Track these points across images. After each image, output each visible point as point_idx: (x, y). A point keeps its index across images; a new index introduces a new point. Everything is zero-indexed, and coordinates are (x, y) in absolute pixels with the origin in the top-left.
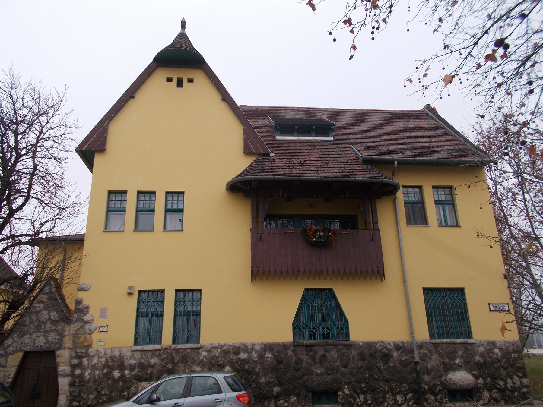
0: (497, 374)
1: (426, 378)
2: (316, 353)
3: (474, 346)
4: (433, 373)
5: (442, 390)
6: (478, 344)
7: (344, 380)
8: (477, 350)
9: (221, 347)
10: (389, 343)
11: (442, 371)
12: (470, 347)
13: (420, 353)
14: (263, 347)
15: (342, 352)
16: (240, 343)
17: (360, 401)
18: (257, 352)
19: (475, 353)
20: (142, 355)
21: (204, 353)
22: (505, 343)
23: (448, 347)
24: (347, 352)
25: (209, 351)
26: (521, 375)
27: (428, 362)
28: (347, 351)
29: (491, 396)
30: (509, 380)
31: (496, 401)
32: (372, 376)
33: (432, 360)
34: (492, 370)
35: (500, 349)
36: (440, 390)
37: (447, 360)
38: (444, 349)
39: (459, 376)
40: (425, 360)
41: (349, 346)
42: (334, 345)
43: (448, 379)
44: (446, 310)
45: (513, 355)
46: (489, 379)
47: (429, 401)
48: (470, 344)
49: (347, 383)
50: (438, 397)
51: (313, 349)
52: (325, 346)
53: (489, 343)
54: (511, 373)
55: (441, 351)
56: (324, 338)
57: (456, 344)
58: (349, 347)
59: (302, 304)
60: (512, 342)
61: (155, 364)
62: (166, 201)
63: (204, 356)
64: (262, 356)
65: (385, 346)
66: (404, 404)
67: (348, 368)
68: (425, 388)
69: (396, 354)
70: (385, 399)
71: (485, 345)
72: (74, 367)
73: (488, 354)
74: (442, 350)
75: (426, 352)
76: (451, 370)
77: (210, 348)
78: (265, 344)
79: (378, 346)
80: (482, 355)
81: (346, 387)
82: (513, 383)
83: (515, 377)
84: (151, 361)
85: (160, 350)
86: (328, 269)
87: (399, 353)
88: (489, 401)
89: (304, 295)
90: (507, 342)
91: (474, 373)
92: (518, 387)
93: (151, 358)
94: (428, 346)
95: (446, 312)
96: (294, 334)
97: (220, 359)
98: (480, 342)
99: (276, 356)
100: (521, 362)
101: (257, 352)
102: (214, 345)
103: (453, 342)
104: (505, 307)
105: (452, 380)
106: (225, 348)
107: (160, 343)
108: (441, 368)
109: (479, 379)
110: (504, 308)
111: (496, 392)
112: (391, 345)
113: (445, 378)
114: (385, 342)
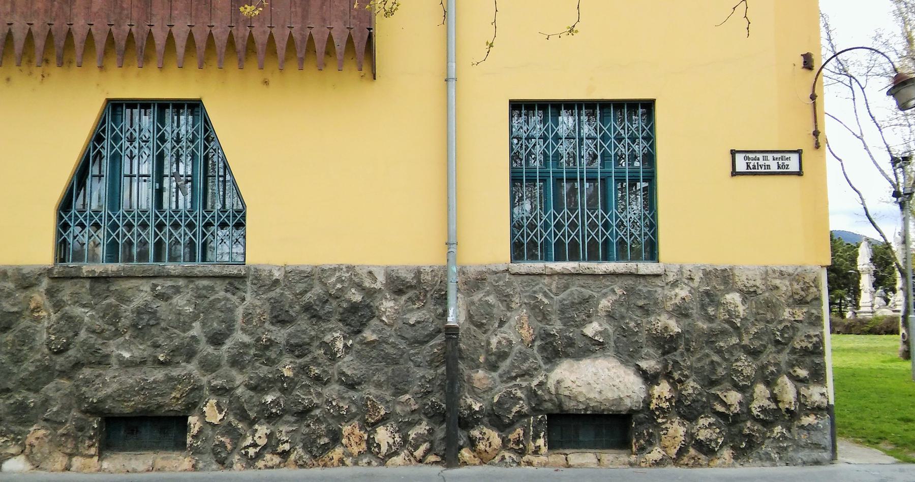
0: (721, 371)
1: (480, 376)
2: (123, 299)
3: (658, 282)
4: (505, 365)
5: (526, 416)
6: (671, 278)
7: (209, 382)
8: (666, 296)
10: (370, 273)
11: (536, 359)
12: (642, 287)
13: (473, 303)
15: (212, 298)
17: (255, 445)
19: (656, 304)
22: (767, 272)
23: (566, 287)
24: (228, 300)
26: (803, 373)
27: (495, 331)
28: (229, 295)
29: (690, 435)
30: (761, 390)
31: (707, 449)
32: (303, 369)
33: (506, 325)
34: (707, 355)
35: (748, 294)
36: (520, 415)
37: (556, 326)
38: (554, 290)
39: (589, 375)
40: (482, 324)
42: (186, 277)
43: (551, 384)
44: (582, 172)
45: (786, 314)
46: (692, 384)
47: (481, 446)
48: (644, 276)
49: (219, 391)
50: (512, 436)
51: (113, 288)
52: (155, 281)
53: (707, 274)
54: (773, 368)
55: (540, 296)
57: (594, 275)
58: (236, 284)
59: (95, 148)
60: (791, 271)
65: (357, 280)
66: (396, 453)
67: (225, 347)
68: (470, 407)
69: (391, 304)
70: (336, 438)
71: (697, 279)
73: (703, 307)
74: (546, 295)
75: (491, 299)
76: (567, 356)
79: (333, 279)
80: (681, 312)
81: (213, 401)
82: (774, 398)
83: (784, 380)
86: (253, 33)
87: (402, 302)
88: (682, 452)
89: (104, 122)
90: (774, 271)
91: (644, 365)
92: (788, 410)
94: (501, 283)
95: (582, 179)
98: (681, 271)
100: (812, 333)
103: (587, 271)
104: (786, 162)
105: (563, 385)
108: (535, 348)
109: (658, 384)
110: (784, 166)
111: (710, 424)
112: (375, 280)
113: (541, 378)
114: (357, 269)
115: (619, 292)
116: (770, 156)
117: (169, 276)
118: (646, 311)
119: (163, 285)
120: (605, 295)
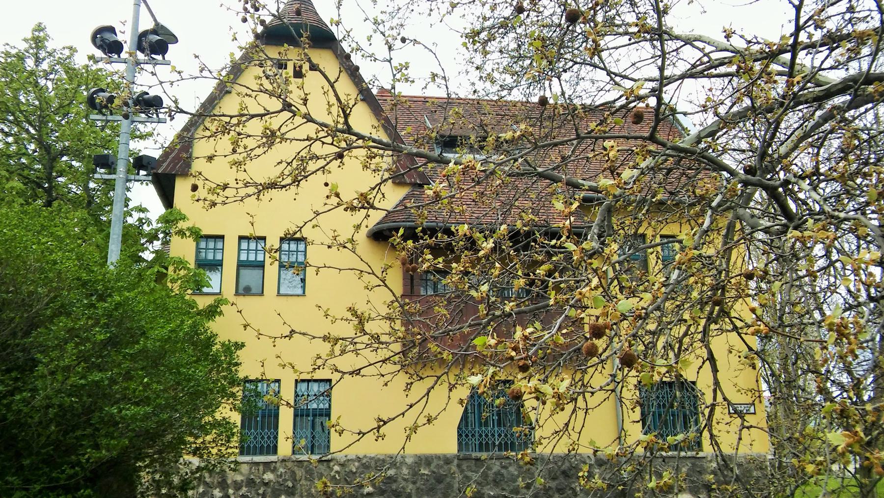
2: (489, 468)
3: (704, 460)
6: (709, 459)
9: (359, 459)
14: (417, 460)
18: (410, 467)
20: (251, 469)
21: (337, 468)
25: (342, 465)
35: (740, 465)
45: (755, 474)
55: (658, 467)
56: (500, 450)
61: (270, 481)
62: (240, 250)
63: (337, 472)
64: (415, 474)
77: (345, 461)
78: (419, 457)
84: (264, 477)
85: (276, 462)
93: (264, 473)
96: (460, 444)
97: (357, 475)
99: (434, 472)
101: (410, 467)
102: (349, 457)
106: (364, 461)
107: (275, 451)
115: (690, 465)
116: (743, 406)
118: (700, 473)
119: (505, 462)
120: (684, 466)
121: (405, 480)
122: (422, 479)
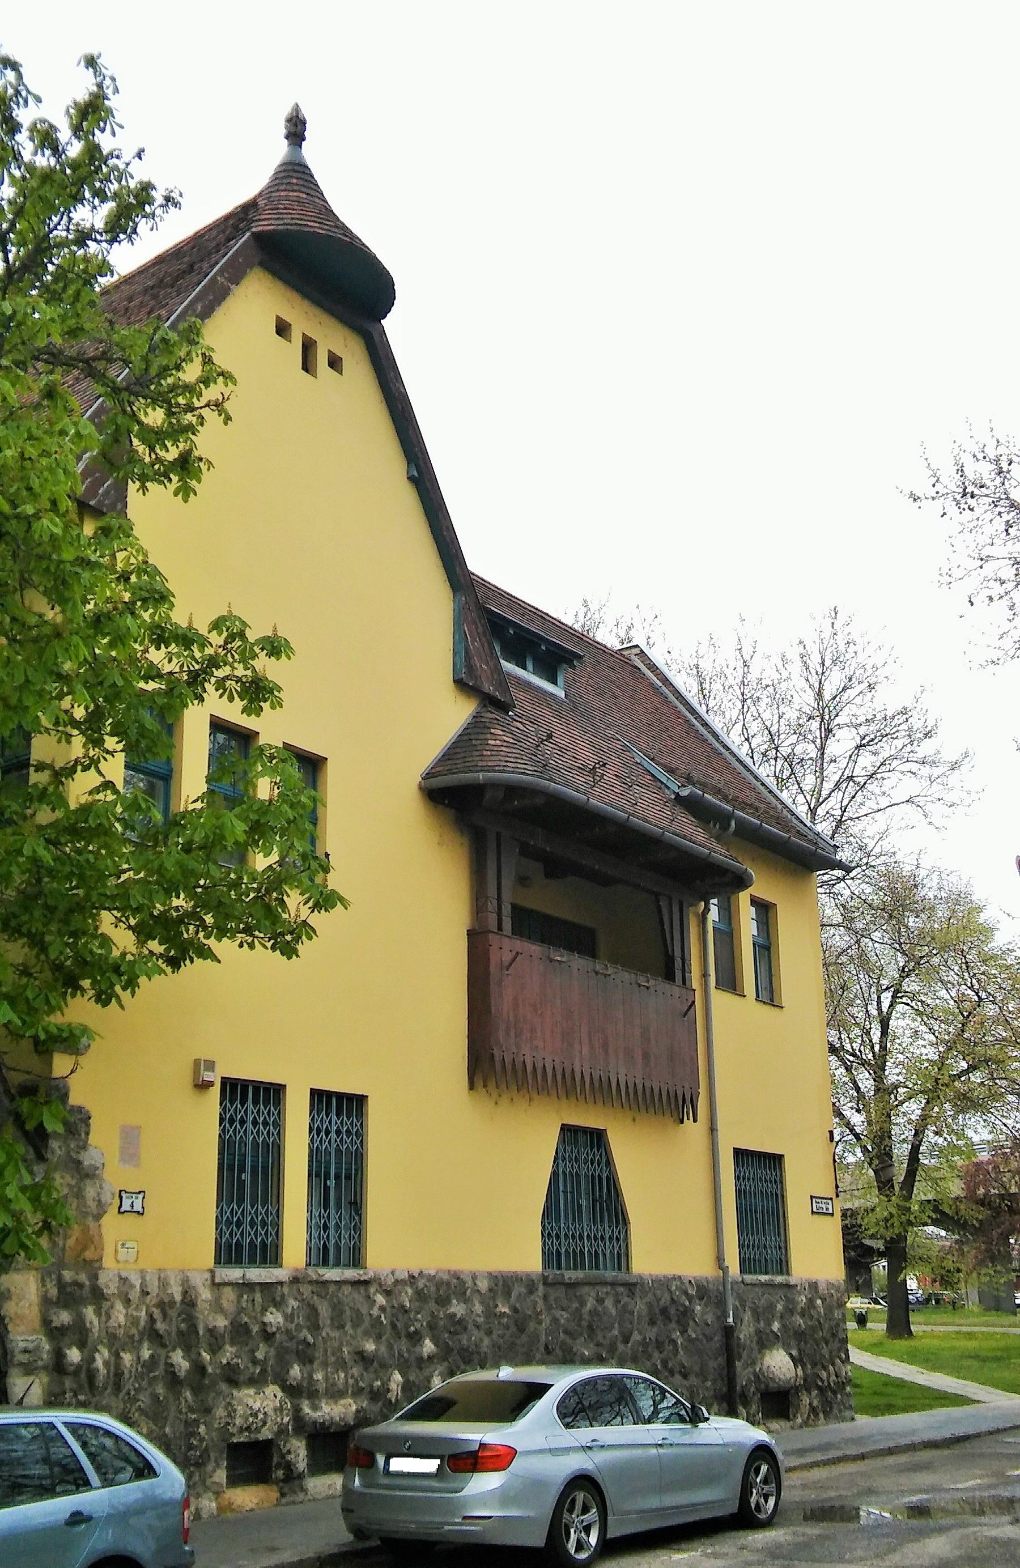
16: (449, 1271)
41: (632, 1287)
64: (490, 1313)
72: (55, 1333)
93: (264, 1310)
106: (420, 1284)
117: (605, 1283)
121: (478, 1327)
122: (499, 1323)
